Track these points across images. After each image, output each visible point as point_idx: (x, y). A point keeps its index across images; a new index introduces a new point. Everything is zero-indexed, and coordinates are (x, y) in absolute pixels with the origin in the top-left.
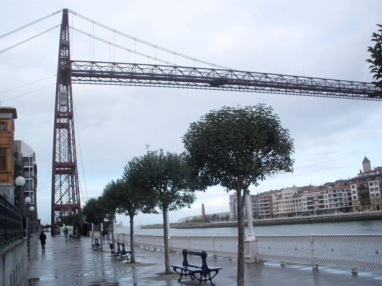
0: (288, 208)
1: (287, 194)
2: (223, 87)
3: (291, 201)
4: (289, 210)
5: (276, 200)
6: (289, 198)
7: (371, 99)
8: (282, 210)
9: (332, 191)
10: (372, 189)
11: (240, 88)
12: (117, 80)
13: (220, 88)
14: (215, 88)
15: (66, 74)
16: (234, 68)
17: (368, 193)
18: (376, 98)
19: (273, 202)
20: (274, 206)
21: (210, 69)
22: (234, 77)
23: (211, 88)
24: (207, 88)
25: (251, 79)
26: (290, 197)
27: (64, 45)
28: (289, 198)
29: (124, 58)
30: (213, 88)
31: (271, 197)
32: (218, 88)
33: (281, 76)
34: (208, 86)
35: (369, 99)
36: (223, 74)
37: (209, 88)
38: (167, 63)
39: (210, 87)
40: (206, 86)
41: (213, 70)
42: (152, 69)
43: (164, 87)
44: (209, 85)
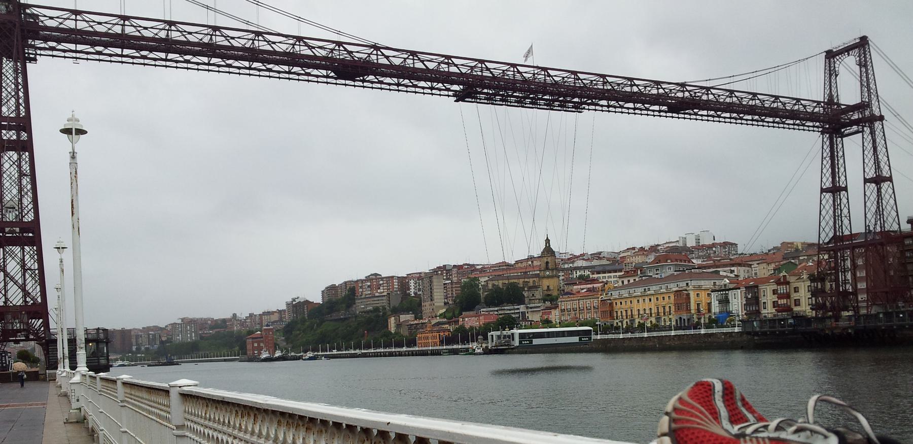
2: (364, 81)
7: (674, 115)
11: (398, 85)
12: (137, 55)
13: (357, 83)
14: (348, 82)
16: (382, 42)
18: (684, 114)
21: (333, 42)
22: (383, 61)
23: (339, 81)
24: (329, 80)
25: (419, 65)
30: (343, 82)
32: (353, 83)
33: (482, 62)
34: (332, 77)
35: (670, 114)
36: (360, 54)
37: (334, 81)
38: (248, 23)
39: (336, 79)
40: (327, 77)
41: (339, 44)
42: (294, 45)
43: (279, 78)
44: (332, 74)
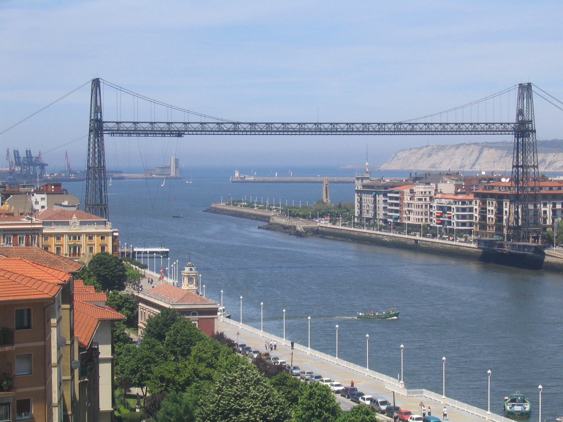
0: (420, 217)
1: (422, 192)
3: (426, 206)
4: (422, 219)
5: (409, 199)
6: (423, 200)
8: (413, 219)
9: (460, 203)
10: (489, 210)
15: (98, 128)
17: (486, 216)
19: (405, 201)
20: (405, 209)
26: (425, 199)
27: (97, 109)
28: (423, 200)
29: (144, 114)
31: (403, 193)
